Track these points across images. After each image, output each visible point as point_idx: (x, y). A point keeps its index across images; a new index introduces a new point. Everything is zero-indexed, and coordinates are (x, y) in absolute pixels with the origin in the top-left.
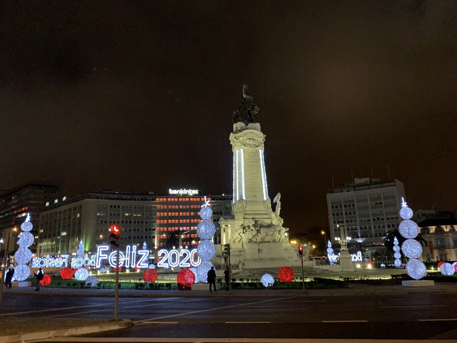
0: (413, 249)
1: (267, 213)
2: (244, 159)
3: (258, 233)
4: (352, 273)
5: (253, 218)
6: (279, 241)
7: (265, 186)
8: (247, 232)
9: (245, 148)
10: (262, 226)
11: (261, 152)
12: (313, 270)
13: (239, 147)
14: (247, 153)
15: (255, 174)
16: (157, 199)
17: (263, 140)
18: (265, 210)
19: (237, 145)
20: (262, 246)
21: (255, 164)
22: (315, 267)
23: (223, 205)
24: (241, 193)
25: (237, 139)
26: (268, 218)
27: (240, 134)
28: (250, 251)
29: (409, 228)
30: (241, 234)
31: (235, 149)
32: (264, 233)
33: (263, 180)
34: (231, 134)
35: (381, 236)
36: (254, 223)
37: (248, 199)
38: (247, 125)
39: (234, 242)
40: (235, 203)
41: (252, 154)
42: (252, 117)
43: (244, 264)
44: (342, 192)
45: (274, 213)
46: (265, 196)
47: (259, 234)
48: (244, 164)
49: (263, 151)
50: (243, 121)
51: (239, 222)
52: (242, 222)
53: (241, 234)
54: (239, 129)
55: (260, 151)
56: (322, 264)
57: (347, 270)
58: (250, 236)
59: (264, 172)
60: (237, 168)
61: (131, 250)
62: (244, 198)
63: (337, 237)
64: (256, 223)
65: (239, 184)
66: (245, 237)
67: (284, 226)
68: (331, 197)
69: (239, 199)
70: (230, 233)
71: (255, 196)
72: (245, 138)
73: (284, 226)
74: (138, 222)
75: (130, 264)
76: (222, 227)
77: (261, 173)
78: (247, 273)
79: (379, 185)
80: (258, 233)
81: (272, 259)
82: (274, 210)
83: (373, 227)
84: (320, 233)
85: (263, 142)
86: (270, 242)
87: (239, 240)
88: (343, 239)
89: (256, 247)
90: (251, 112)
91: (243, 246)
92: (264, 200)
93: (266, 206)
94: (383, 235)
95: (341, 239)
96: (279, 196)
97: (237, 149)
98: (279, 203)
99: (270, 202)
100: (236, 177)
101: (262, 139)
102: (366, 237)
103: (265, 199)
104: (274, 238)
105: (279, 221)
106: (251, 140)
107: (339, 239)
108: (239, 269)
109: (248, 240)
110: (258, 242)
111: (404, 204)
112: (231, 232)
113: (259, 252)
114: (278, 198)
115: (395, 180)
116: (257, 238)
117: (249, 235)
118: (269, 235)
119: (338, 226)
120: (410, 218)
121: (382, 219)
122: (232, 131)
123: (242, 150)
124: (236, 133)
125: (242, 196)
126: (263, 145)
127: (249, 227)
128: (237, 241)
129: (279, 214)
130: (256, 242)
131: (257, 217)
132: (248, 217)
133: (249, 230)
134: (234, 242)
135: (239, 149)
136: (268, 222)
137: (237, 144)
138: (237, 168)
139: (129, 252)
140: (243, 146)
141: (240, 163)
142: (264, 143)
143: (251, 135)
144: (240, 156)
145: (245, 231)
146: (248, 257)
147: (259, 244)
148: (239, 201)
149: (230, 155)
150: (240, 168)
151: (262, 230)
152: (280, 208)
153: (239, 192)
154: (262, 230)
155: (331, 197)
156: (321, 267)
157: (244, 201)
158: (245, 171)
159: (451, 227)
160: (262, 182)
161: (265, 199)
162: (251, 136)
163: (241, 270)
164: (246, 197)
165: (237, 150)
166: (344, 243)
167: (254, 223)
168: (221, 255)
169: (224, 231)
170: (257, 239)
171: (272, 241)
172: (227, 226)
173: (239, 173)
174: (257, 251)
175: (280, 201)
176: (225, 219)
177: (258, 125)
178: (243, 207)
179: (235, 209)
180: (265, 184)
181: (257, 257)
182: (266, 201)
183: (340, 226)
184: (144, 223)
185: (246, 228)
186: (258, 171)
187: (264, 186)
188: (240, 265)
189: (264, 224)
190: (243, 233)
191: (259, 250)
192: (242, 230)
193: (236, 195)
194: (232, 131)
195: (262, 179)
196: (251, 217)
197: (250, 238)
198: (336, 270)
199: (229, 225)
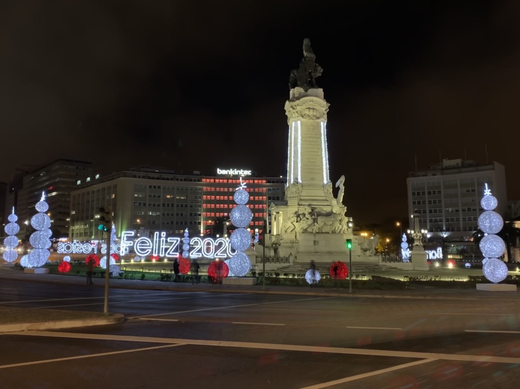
0: (492, 247)
1: (327, 199)
2: (301, 134)
3: (314, 222)
4: (422, 273)
5: (309, 205)
6: (340, 232)
7: (326, 167)
8: (301, 221)
9: (304, 120)
10: (319, 214)
11: (323, 125)
12: (377, 267)
14: (306, 124)
15: (314, 152)
16: (204, 180)
17: (326, 110)
19: (294, 116)
20: (318, 237)
21: (315, 140)
22: (381, 263)
23: (280, 189)
24: (296, 175)
25: (294, 109)
26: (328, 205)
27: (297, 102)
28: (305, 243)
29: (491, 222)
30: (295, 223)
31: (291, 121)
32: (322, 222)
33: (324, 159)
34: (287, 103)
35: (471, 230)
36: (310, 211)
37: (304, 183)
38: (306, 91)
39: (286, 231)
40: (289, 187)
41: (312, 127)
42: (314, 80)
43: (296, 257)
44: (426, 175)
45: (335, 199)
46: (326, 180)
47: (315, 224)
48: (302, 139)
49: (325, 124)
50: (301, 86)
51: (292, 209)
52: (296, 209)
53: (295, 223)
54: (296, 95)
55: (322, 123)
56: (391, 260)
57: (420, 269)
58: (305, 226)
59: (325, 149)
60: (293, 144)
62: (300, 181)
63: (411, 230)
64: (312, 210)
65: (294, 164)
66: (299, 227)
67: (347, 215)
68: (412, 182)
69: (294, 181)
70: (281, 222)
71: (313, 179)
72: (304, 107)
73: (347, 215)
74: (182, 206)
76: (273, 215)
77: (322, 151)
78: (299, 267)
79: (473, 169)
80: (314, 222)
81: (330, 253)
82: (336, 195)
83: (461, 219)
84: (395, 224)
85: (326, 113)
86: (328, 233)
87: (291, 230)
88: (417, 232)
89: (312, 238)
90: (313, 74)
91: (296, 236)
92: (324, 184)
93: (326, 191)
94: (473, 229)
95: (415, 232)
96: (342, 179)
97: (293, 121)
98: (342, 188)
99: (331, 186)
100: (291, 156)
101: (325, 109)
102: (453, 230)
103: (325, 182)
104: (334, 228)
105: (341, 209)
106: (311, 110)
107: (413, 232)
108: (289, 262)
109: (302, 230)
110: (314, 232)
111: (487, 192)
112: (283, 220)
113: (314, 244)
114: (341, 182)
115: (494, 162)
116: (313, 228)
117: (303, 224)
118: (327, 225)
119: (412, 216)
120: (493, 208)
121: (473, 210)
122: (288, 98)
123: (299, 122)
124: (293, 101)
125: (297, 179)
126: (326, 116)
127: (304, 215)
128: (289, 231)
129: (341, 201)
130: (312, 233)
131: (314, 203)
132: (303, 203)
133: (304, 219)
134: (286, 231)
135: (296, 121)
136: (328, 209)
137: (294, 114)
138: (293, 144)
140: (301, 118)
142: (328, 113)
143: (311, 103)
144: (296, 129)
145: (299, 219)
146: (301, 249)
147: (315, 235)
148: (294, 184)
149: (285, 128)
151: (320, 219)
152: (343, 194)
154: (320, 219)
155: (412, 182)
156: (389, 264)
157: (299, 185)
160: (322, 162)
161: (325, 182)
162: (311, 105)
163: (291, 264)
164: (302, 180)
166: (418, 237)
167: (310, 211)
168: (270, 246)
169: (275, 219)
170: (313, 229)
171: (330, 232)
172: (278, 213)
173: (294, 151)
174: (312, 243)
175: (344, 185)
176: (276, 205)
177: (320, 91)
178: (297, 192)
179: (288, 194)
180: (326, 165)
181: (312, 249)
183: (414, 217)
184: (189, 206)
185: (301, 216)
186: (318, 149)
187: (324, 167)
188: (291, 259)
189: (323, 212)
190: (297, 222)
191: (315, 242)
192: (296, 218)
193: (291, 178)
194: (288, 98)
195: (322, 158)
196: (307, 203)
197: (305, 228)
198: (406, 269)
199: (280, 212)
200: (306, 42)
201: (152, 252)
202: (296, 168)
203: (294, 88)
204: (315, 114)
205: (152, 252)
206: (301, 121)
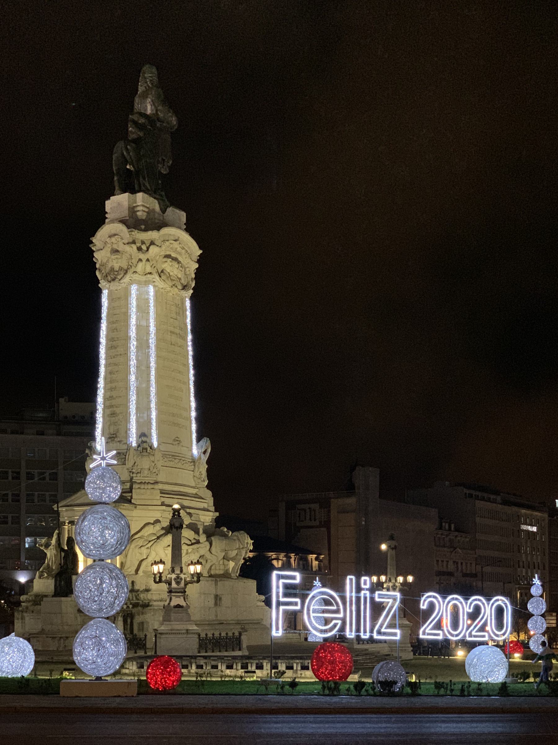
1: (200, 494)
11: (188, 304)
13: (144, 278)
18: (193, 484)
41: (173, 308)
61: (359, 589)
75: (358, 630)
92: (192, 455)
93: (197, 474)
97: (131, 283)
123: (151, 289)
132: (167, 501)
139: (354, 594)
141: (143, 330)
142: (195, 278)
150: (143, 345)
153: (137, 422)
158: (158, 357)
159: (286, 556)
165: (134, 289)
182: (200, 458)
202: (144, 408)
204: (180, 276)
206: (155, 286)
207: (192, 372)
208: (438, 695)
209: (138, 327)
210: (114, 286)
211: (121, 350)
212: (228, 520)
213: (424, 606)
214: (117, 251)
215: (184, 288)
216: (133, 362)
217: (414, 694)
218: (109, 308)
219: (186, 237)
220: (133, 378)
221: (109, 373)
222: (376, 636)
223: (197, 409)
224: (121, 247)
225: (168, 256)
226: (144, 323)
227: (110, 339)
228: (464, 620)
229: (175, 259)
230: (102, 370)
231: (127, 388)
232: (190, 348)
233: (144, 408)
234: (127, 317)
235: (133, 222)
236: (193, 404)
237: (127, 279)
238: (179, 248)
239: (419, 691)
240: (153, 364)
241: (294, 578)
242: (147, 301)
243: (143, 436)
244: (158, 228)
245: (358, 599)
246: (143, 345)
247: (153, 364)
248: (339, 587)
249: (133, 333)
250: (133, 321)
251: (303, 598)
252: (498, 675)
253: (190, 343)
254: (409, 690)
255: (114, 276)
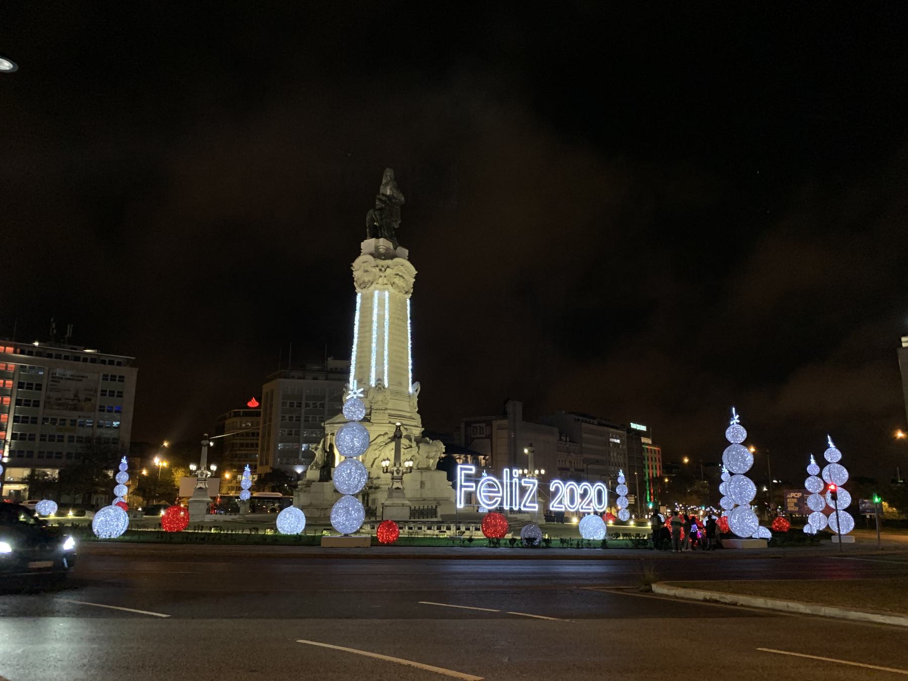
11: (408, 302)
13: (382, 287)
25: (380, 270)
38: (395, 249)
61: (511, 477)
97: (376, 289)
123: (387, 293)
132: (393, 421)
141: (381, 317)
143: (402, 268)
150: (381, 326)
158: (390, 333)
165: (376, 293)
200: (389, 174)
201: (501, 503)
203: (378, 237)
205: (501, 503)
207: (410, 342)
208: (563, 548)
209: (379, 315)
210: (365, 291)
211: (367, 329)
212: (430, 433)
213: (552, 489)
214: (367, 271)
215: (406, 293)
216: (374, 336)
217: (548, 547)
218: (362, 304)
219: (408, 264)
220: (374, 345)
221: (360, 342)
222: (523, 509)
223: (413, 364)
224: (370, 269)
225: (397, 274)
226: (382, 313)
227: (361, 322)
228: (577, 499)
229: (401, 276)
230: (355, 341)
231: (370, 352)
232: (409, 328)
233: (380, 363)
234: (371, 309)
235: (377, 255)
236: (410, 362)
237: (372, 288)
238: (404, 270)
239: (551, 545)
240: (386, 338)
241: (471, 470)
242: (384, 300)
243: (379, 380)
244: (392, 257)
245: (511, 484)
246: (381, 326)
247: (386, 338)
248: (499, 476)
249: (375, 318)
250: (375, 311)
251: (477, 482)
252: (600, 535)
253: (409, 325)
254: (544, 544)
255: (364, 285)
